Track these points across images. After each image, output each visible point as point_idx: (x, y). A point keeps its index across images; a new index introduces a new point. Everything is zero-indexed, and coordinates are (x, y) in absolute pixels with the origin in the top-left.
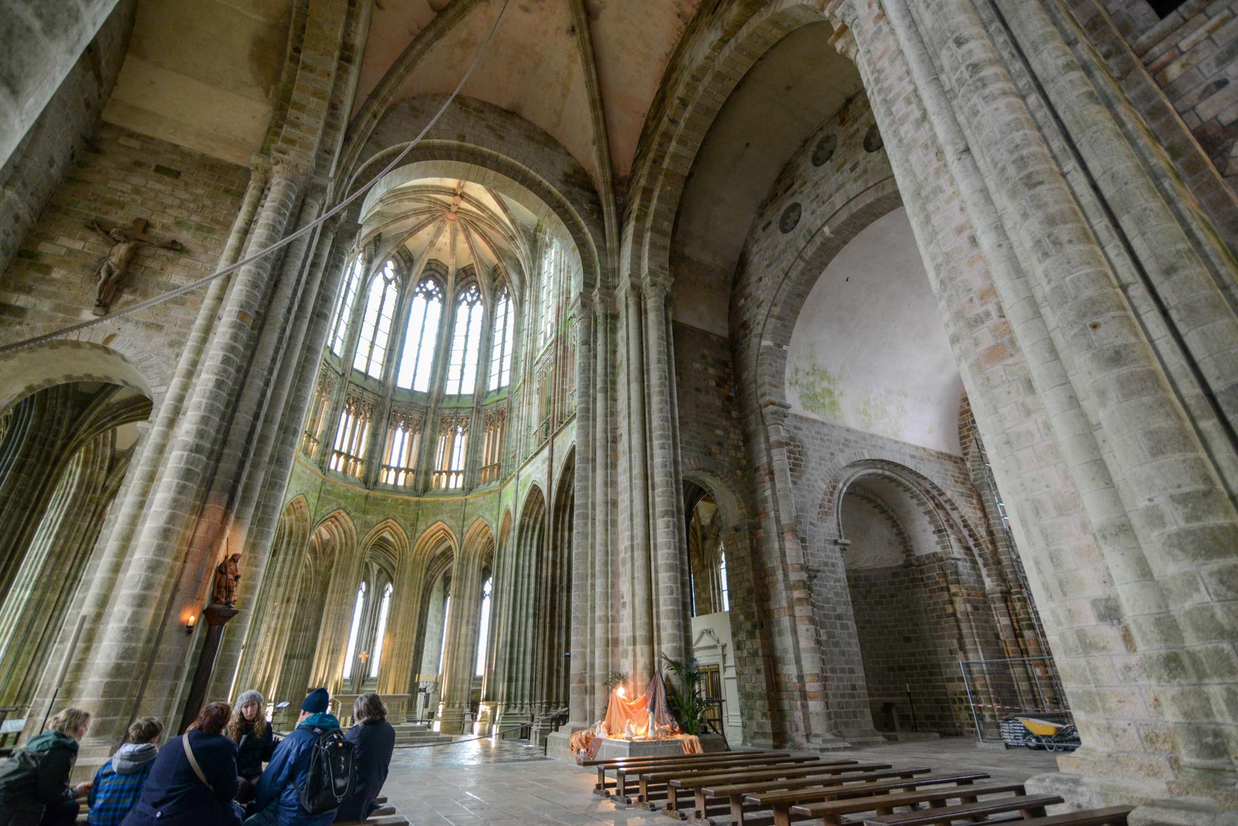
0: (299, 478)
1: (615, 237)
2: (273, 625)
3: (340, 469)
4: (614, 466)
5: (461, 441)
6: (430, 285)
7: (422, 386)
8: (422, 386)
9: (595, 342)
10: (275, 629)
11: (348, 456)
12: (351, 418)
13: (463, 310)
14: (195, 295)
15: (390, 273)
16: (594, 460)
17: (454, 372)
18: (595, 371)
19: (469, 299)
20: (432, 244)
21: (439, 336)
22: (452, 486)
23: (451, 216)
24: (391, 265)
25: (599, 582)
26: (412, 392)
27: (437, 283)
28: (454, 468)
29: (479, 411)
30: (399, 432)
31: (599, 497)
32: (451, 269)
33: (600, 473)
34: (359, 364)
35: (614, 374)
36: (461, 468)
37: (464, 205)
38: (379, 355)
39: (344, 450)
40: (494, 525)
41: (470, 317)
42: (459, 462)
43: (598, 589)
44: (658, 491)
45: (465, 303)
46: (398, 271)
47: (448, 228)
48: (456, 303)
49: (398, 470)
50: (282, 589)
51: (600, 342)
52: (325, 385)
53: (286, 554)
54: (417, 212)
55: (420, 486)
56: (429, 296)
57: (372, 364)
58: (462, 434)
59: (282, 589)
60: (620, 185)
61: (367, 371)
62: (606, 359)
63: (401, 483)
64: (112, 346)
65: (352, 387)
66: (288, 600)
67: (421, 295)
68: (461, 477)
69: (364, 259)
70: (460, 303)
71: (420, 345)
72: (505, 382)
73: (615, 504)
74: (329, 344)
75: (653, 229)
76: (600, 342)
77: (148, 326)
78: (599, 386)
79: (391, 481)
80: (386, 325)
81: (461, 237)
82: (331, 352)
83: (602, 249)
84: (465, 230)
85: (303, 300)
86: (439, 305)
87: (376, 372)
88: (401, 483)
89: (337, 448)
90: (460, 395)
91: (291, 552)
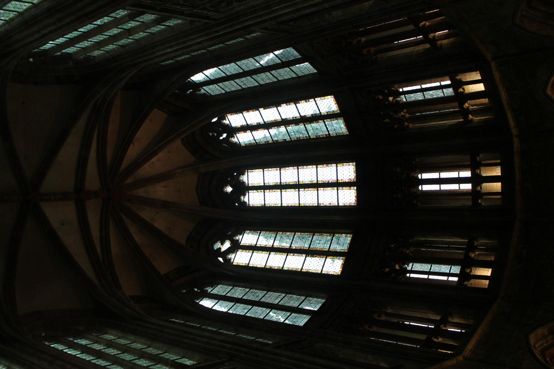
3: (488, 272)
7: (347, 171)
8: (347, 171)
11: (467, 264)
13: (244, 138)
15: (227, 245)
17: (317, 129)
20: (165, 205)
21: (281, 164)
22: (480, 87)
24: (218, 245)
28: (449, 92)
34: (334, 267)
38: (321, 242)
39: (456, 269)
42: (437, 88)
45: (235, 140)
47: (141, 192)
49: (476, 180)
57: (336, 247)
63: (497, 172)
69: (213, 284)
79: (497, 186)
81: (147, 170)
87: (343, 242)
88: (497, 172)
90: (343, 113)
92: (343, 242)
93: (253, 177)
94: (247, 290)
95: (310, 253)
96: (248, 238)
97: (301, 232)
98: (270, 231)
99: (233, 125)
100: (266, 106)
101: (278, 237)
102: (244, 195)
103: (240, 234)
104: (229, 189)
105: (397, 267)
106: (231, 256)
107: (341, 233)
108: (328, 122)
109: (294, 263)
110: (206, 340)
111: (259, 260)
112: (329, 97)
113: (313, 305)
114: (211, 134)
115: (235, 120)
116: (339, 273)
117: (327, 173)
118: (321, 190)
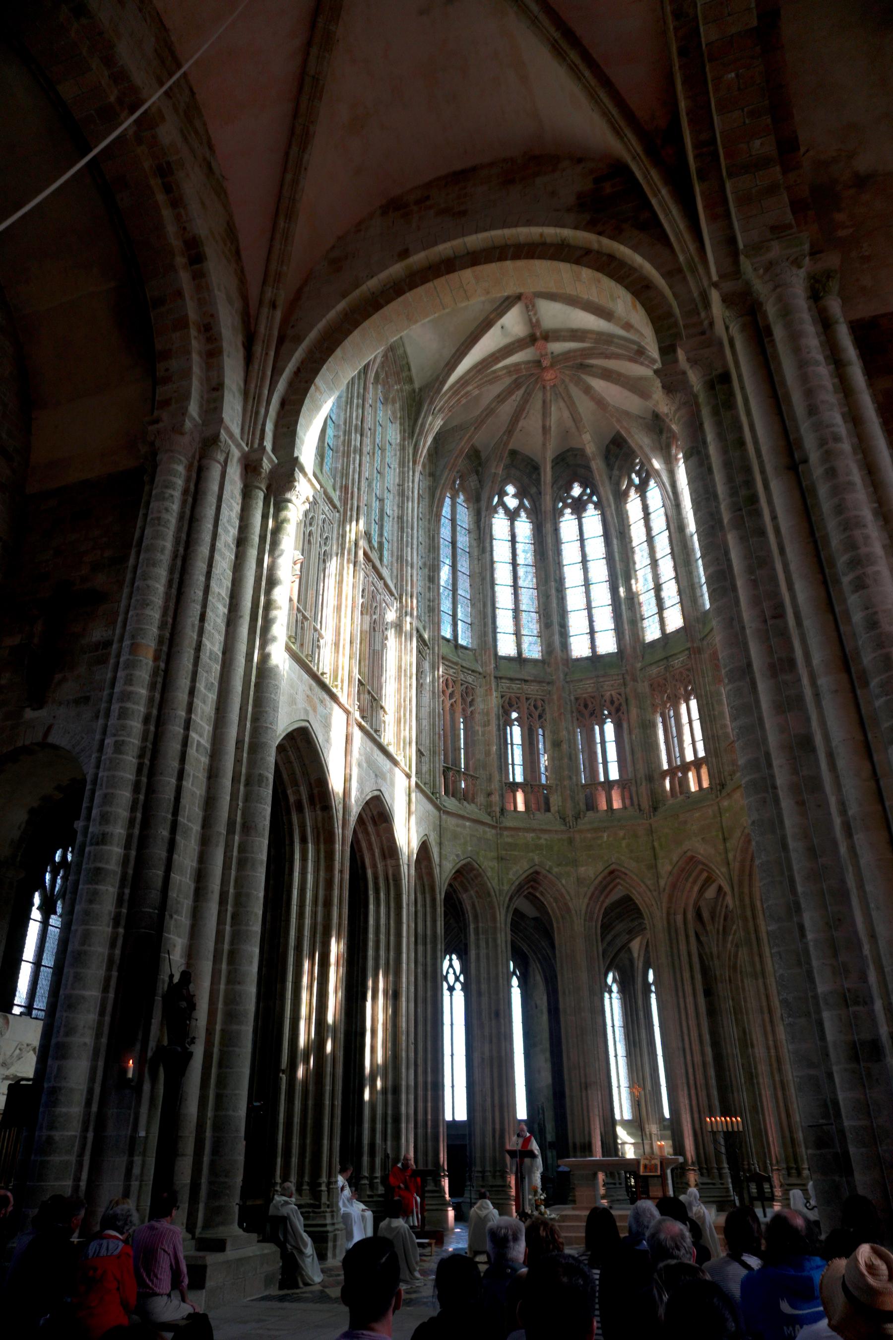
0: (455, 836)
1: (687, 237)
2: (487, 1053)
5: (690, 711)
7: (607, 644)
8: (607, 644)
10: (491, 1058)
13: (633, 506)
14: (108, 644)
15: (512, 502)
16: (749, 665)
18: (716, 496)
19: (637, 481)
22: (693, 787)
23: (548, 375)
24: (511, 489)
26: (595, 659)
27: (584, 486)
28: (689, 757)
29: (699, 651)
31: (773, 740)
32: (590, 449)
33: (763, 686)
35: (749, 483)
36: (701, 754)
37: (557, 347)
38: (531, 624)
43: (810, 936)
48: (621, 497)
50: (485, 999)
51: (710, 437)
53: (478, 947)
54: (501, 398)
55: (645, 805)
57: (526, 642)
59: (485, 999)
60: (661, 144)
62: (727, 465)
63: (617, 804)
64: (50, 740)
65: (505, 684)
66: (497, 1014)
67: (568, 511)
68: (704, 771)
70: (626, 494)
75: (730, 175)
76: (710, 437)
77: (77, 702)
78: (726, 517)
80: (527, 579)
82: (457, 646)
83: (673, 273)
84: (578, 382)
87: (533, 650)
91: (483, 944)
92: (533, 650)
93: (592, 519)
94: (467, 550)
95: (517, 611)
96: (524, 528)
97: (538, 596)
99: (649, 494)
101: (530, 569)
102: (572, 513)
103: (527, 518)
104: (576, 491)
105: (514, 715)
106: (501, 511)
107: (541, 646)
109: (504, 597)
110: (409, 559)
111: (501, 551)
112: (682, 621)
114: (637, 461)
115: (654, 495)
116: (500, 654)
117: (605, 619)
118: (586, 613)
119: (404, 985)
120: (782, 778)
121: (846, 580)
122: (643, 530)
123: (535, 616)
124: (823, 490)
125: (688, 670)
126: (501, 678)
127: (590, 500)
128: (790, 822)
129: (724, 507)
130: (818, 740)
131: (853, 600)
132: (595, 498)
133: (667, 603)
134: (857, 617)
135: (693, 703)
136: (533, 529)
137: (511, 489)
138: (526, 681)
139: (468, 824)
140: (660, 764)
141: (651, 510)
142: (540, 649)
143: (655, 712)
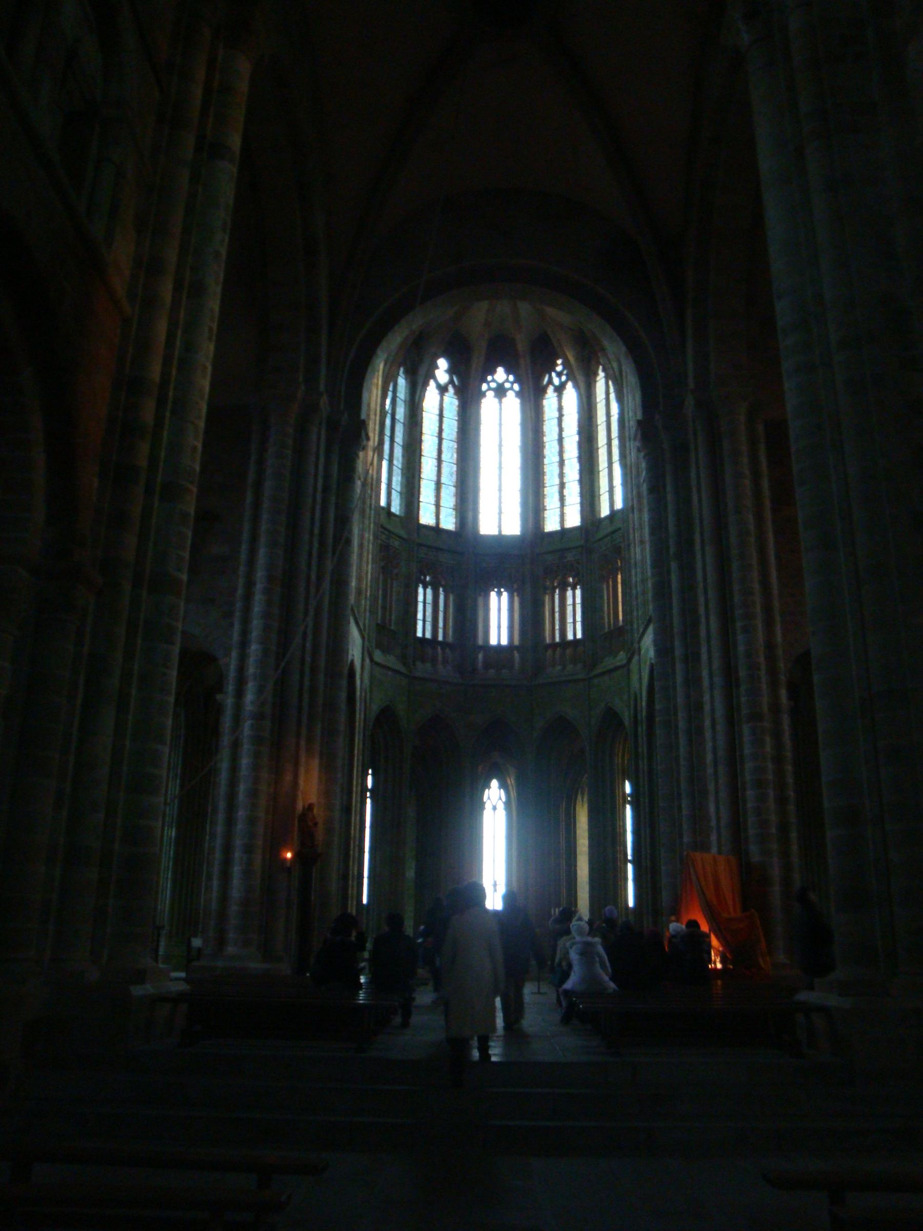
4: (697, 657)
5: (575, 598)
6: (500, 374)
7: (513, 527)
8: (513, 527)
9: (664, 487)
12: (429, 591)
19: (556, 381)
24: (442, 364)
25: (685, 803)
30: (493, 595)
31: (680, 700)
34: (426, 517)
38: (449, 498)
40: (626, 714)
41: (560, 409)
43: (685, 812)
44: (743, 688)
45: (551, 389)
46: (451, 371)
48: (540, 392)
51: (669, 488)
52: (387, 557)
56: (500, 392)
58: (574, 589)
61: (438, 523)
67: (490, 394)
71: (500, 468)
72: (619, 505)
73: (699, 707)
74: (383, 503)
78: (672, 550)
85: (323, 533)
86: (517, 402)
87: (448, 523)
89: (419, 634)
95: (438, 485)
96: (451, 402)
97: (457, 471)
98: (458, 433)
100: (580, 444)
104: (500, 374)
105: (428, 578)
108: (558, 511)
113: (396, 508)
114: (559, 362)
119: (354, 803)
120: (682, 725)
121: (739, 624)
122: (557, 429)
123: (453, 490)
124: (735, 565)
125: (578, 563)
126: (421, 545)
127: (512, 389)
128: (683, 750)
129: (672, 542)
130: (707, 708)
131: (740, 638)
132: (516, 387)
133: (568, 501)
134: (741, 649)
135: (578, 592)
136: (459, 406)
137: (442, 364)
138: (441, 550)
139: (390, 673)
140: (544, 638)
141: (565, 412)
142: (454, 520)
143: (545, 593)
